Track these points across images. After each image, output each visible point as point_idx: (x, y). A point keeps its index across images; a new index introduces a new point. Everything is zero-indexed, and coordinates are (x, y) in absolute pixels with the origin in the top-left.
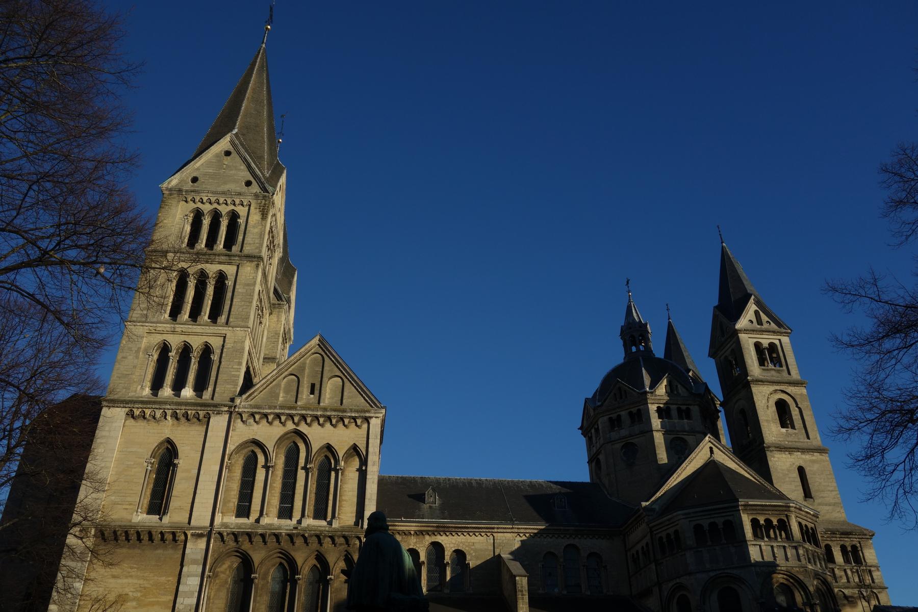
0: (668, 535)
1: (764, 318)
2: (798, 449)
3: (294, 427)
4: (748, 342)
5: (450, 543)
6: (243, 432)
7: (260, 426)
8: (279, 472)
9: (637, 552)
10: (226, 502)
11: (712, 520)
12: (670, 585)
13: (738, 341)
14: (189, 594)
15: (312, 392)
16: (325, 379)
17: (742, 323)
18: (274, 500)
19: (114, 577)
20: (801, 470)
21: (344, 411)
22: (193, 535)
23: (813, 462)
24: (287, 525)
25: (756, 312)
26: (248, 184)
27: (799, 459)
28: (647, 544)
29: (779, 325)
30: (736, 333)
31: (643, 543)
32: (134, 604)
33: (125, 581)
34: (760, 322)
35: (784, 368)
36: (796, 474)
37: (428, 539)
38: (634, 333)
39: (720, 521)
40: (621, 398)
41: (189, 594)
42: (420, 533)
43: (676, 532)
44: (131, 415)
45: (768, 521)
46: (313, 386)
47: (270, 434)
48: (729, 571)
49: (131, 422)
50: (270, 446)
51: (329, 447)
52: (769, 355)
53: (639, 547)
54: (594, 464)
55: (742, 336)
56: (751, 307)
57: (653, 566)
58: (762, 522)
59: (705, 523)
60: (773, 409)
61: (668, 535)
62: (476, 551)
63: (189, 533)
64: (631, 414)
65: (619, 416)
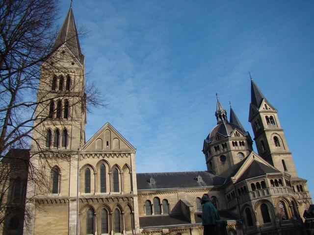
0: (242, 188)
1: (268, 107)
2: (282, 154)
4: (263, 116)
5: (162, 197)
6: (83, 162)
7: (89, 159)
8: (99, 175)
10: (81, 187)
12: (243, 205)
13: (260, 116)
14: (74, 221)
15: (108, 145)
16: (112, 139)
17: (261, 109)
18: (99, 186)
19: (45, 216)
20: (283, 161)
21: (121, 151)
22: (71, 200)
24: (105, 195)
25: (265, 105)
27: (282, 157)
28: (233, 192)
29: (274, 109)
30: (259, 113)
31: (232, 191)
32: (54, 225)
33: (49, 218)
34: (267, 109)
35: (276, 125)
36: (281, 163)
37: (154, 196)
38: (218, 115)
39: (260, 182)
41: (74, 221)
42: (151, 194)
43: (245, 187)
45: (276, 180)
46: (107, 142)
47: (94, 161)
48: (265, 198)
50: (94, 166)
51: (116, 165)
52: (270, 120)
53: (230, 193)
54: (209, 164)
55: (261, 114)
56: (264, 103)
57: (236, 199)
58: (274, 181)
59: (255, 183)
60: (273, 140)
61: (242, 188)
63: (69, 199)
65: (218, 146)
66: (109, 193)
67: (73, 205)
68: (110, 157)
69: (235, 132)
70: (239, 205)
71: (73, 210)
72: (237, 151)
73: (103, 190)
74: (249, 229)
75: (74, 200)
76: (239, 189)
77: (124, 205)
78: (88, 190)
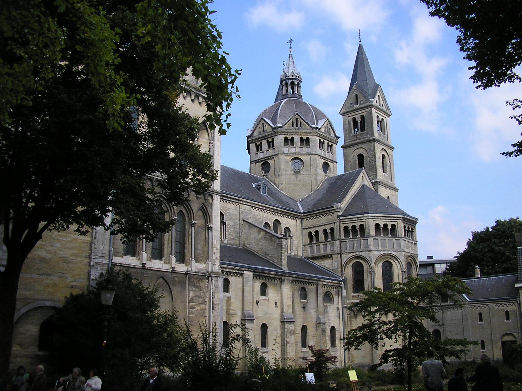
0: (354, 227)
9: (317, 232)
11: (385, 223)
12: (350, 255)
23: (393, 195)
28: (332, 229)
35: (386, 136)
39: (389, 225)
40: (297, 126)
43: (362, 226)
55: (374, 110)
64: (301, 139)
65: (293, 139)
69: (325, 124)
70: (341, 254)
72: (323, 158)
74: (353, 296)
76: (346, 228)
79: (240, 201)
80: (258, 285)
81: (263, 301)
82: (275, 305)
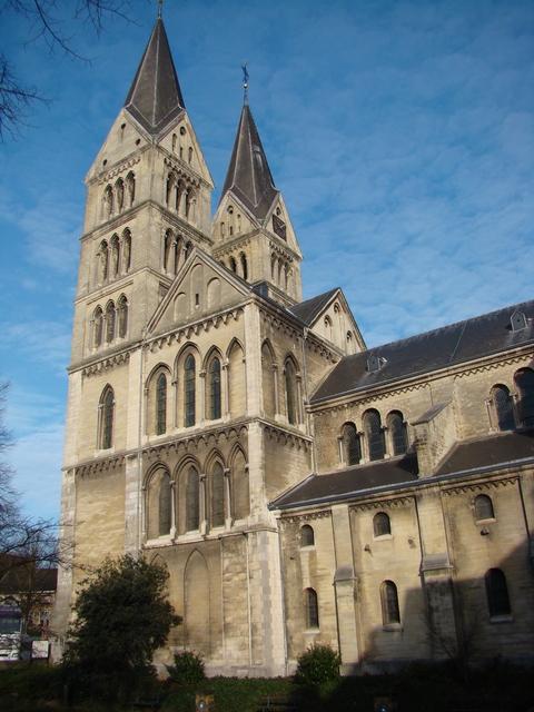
3: (186, 340)
5: (383, 405)
6: (155, 358)
10: (147, 424)
14: (132, 507)
15: (197, 303)
18: (182, 413)
19: (90, 502)
26: (138, 142)
37: (362, 408)
41: (132, 507)
42: (353, 403)
44: (84, 374)
46: (197, 295)
47: (168, 354)
49: (86, 379)
50: (171, 364)
51: (214, 349)
62: (412, 407)
66: (203, 424)
67: (134, 468)
68: (202, 332)
71: (132, 480)
73: (191, 421)
75: (133, 458)
77: (226, 448)
78: (161, 428)
79: (426, 377)
80: (366, 520)
81: (381, 544)
82: (408, 546)
